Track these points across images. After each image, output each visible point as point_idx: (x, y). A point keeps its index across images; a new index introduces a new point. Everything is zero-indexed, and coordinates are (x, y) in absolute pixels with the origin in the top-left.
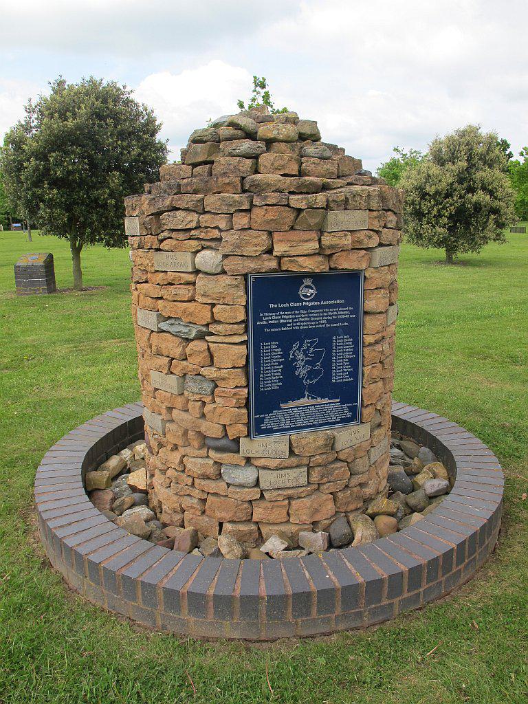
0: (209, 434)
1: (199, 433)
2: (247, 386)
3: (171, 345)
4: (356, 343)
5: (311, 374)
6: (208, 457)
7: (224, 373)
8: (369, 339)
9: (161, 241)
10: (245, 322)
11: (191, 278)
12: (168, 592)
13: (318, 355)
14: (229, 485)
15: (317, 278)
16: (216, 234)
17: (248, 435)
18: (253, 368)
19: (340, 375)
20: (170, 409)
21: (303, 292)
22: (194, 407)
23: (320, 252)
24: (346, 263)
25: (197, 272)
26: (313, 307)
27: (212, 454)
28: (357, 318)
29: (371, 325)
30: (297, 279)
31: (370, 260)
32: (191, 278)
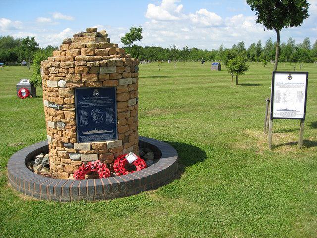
0: (64, 141)
1: (62, 142)
2: (75, 125)
3: (52, 112)
4: (114, 110)
5: (99, 120)
6: (65, 150)
7: (68, 121)
8: (119, 110)
9: (49, 77)
10: (74, 103)
11: (57, 89)
12: (31, 184)
13: (100, 115)
14: (72, 160)
15: (99, 89)
16: (64, 75)
17: (77, 142)
18: (77, 118)
19: (109, 121)
20: (53, 134)
21: (94, 94)
22: (60, 133)
23: (98, 80)
24: (108, 84)
25: (59, 87)
26: (98, 99)
27: (66, 149)
28: (114, 103)
29: (120, 107)
30: (92, 90)
31: (119, 83)
32: (57, 89)
